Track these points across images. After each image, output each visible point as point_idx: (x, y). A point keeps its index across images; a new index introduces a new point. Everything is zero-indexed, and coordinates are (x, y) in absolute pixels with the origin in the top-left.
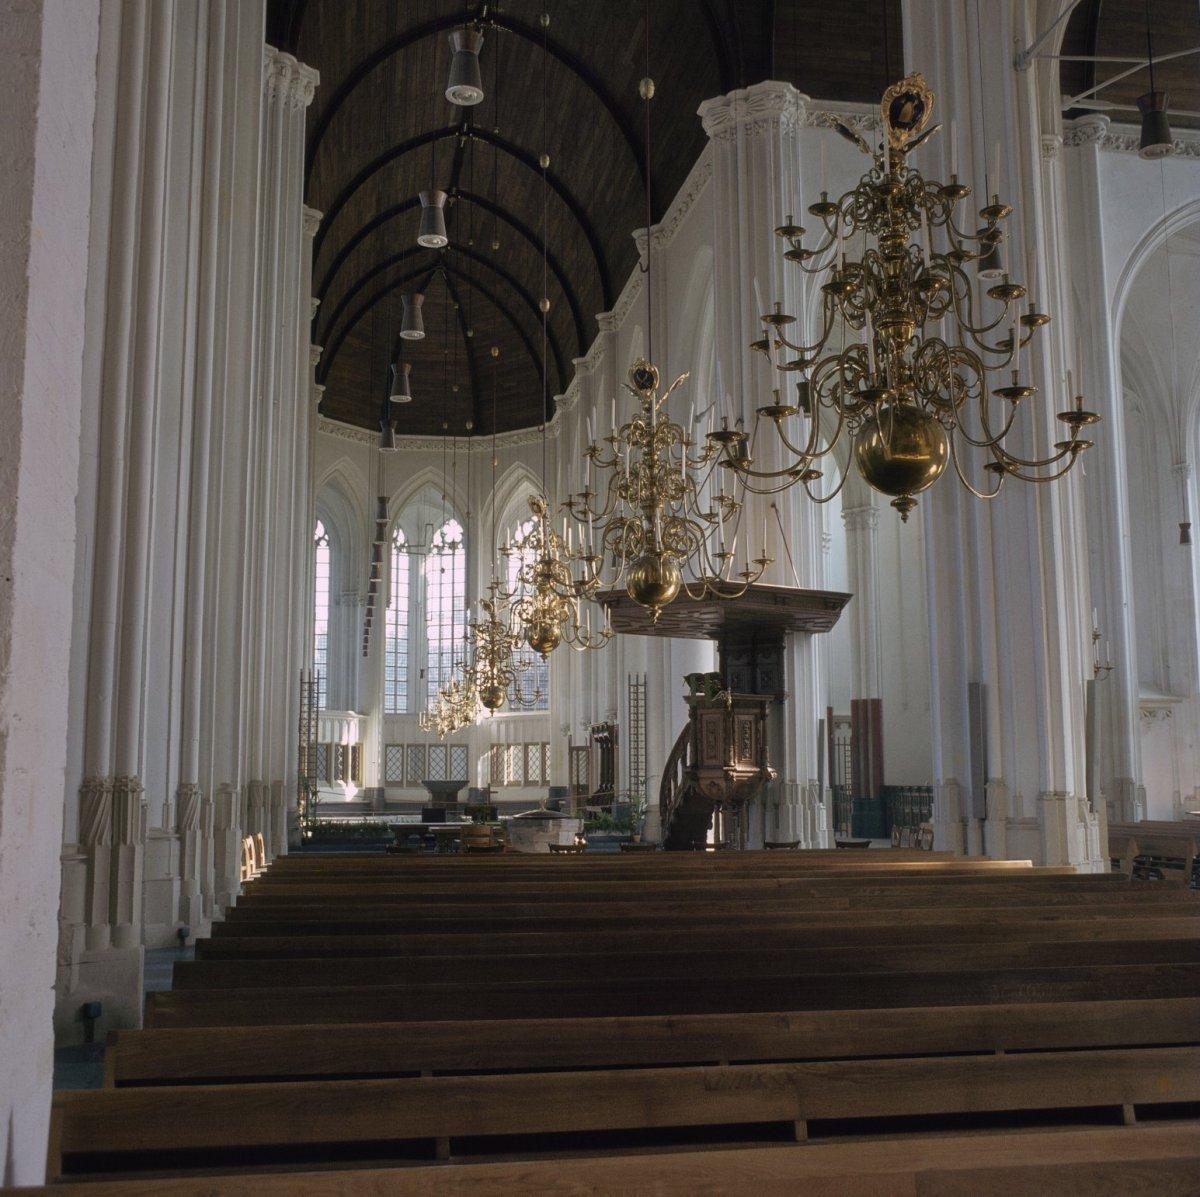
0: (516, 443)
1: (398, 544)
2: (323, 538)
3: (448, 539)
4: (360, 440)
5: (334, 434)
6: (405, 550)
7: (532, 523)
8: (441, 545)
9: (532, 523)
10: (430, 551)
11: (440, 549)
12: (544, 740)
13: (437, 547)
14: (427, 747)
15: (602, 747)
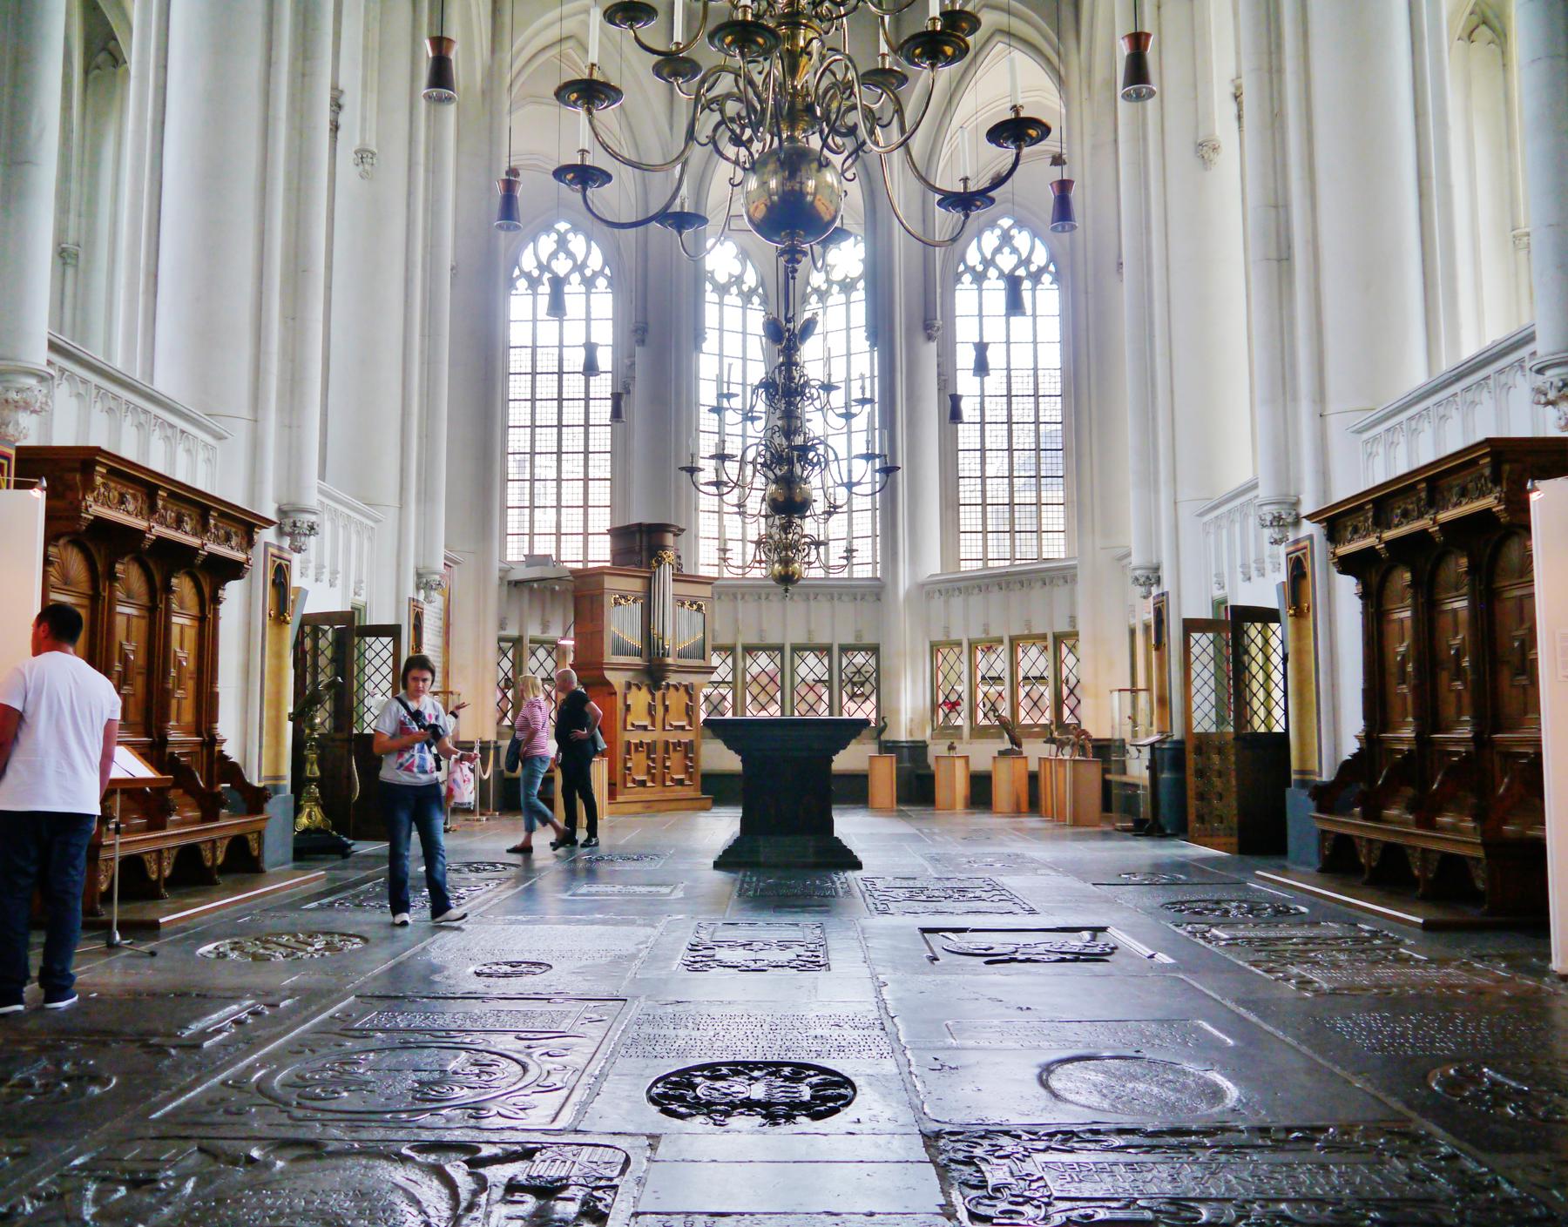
1: (745, 288)
2: (601, 272)
3: (837, 275)
6: (756, 300)
7: (998, 232)
8: (824, 287)
9: (998, 232)
12: (1062, 627)
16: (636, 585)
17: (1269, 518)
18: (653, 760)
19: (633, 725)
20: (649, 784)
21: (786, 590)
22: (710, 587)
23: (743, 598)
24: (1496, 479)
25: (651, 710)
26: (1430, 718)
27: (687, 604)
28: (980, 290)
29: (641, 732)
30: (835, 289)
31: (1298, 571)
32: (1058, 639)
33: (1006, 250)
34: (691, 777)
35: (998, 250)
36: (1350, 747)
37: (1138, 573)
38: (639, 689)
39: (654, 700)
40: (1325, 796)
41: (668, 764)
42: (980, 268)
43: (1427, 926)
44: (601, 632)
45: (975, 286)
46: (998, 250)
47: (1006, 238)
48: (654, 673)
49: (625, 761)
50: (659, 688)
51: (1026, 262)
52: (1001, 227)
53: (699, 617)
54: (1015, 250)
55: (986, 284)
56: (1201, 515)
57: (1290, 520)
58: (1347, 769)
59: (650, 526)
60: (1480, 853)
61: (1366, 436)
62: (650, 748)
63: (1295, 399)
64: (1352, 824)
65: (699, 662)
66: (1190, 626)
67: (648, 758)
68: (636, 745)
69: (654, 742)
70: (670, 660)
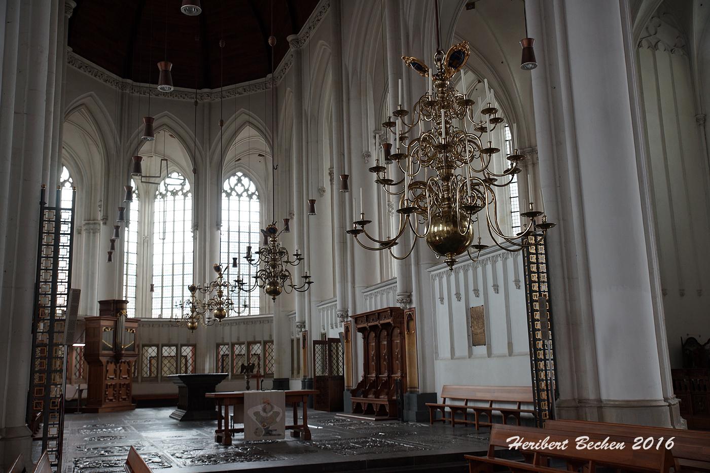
0: (240, 94)
2: (68, 180)
3: (170, 188)
4: (106, 81)
5: (82, 71)
7: (236, 178)
8: (164, 192)
9: (236, 178)
10: (155, 197)
11: (163, 196)
12: (267, 338)
13: (161, 194)
14: (160, 346)
15: (366, 339)
16: (110, 323)
17: (340, 315)
18: (115, 391)
19: (109, 377)
20: (114, 400)
21: (192, 332)
22: (137, 324)
23: (143, 326)
24: (391, 316)
25: (115, 371)
26: (379, 372)
27: (129, 331)
28: (229, 200)
29: (112, 380)
30: (169, 194)
31: (347, 329)
32: (265, 343)
33: (239, 185)
34: (128, 397)
35: (236, 185)
36: (360, 379)
37: (298, 324)
38: (111, 363)
39: (116, 367)
40: (354, 393)
41: (121, 392)
42: (229, 191)
43: (375, 420)
44: (99, 341)
45: (227, 198)
46: (236, 185)
47: (239, 180)
48: (117, 355)
49: (106, 391)
50: (118, 363)
51: (247, 190)
52: (237, 176)
53: (133, 334)
54: (243, 185)
55: (231, 197)
56: (318, 306)
57: (345, 316)
58: (361, 385)
59: (117, 301)
60: (387, 403)
61: (365, 294)
62: (114, 386)
63: (347, 282)
64: (361, 399)
65: (132, 352)
66: (315, 342)
67: (114, 390)
68: (110, 385)
69: (116, 384)
70: (123, 352)
